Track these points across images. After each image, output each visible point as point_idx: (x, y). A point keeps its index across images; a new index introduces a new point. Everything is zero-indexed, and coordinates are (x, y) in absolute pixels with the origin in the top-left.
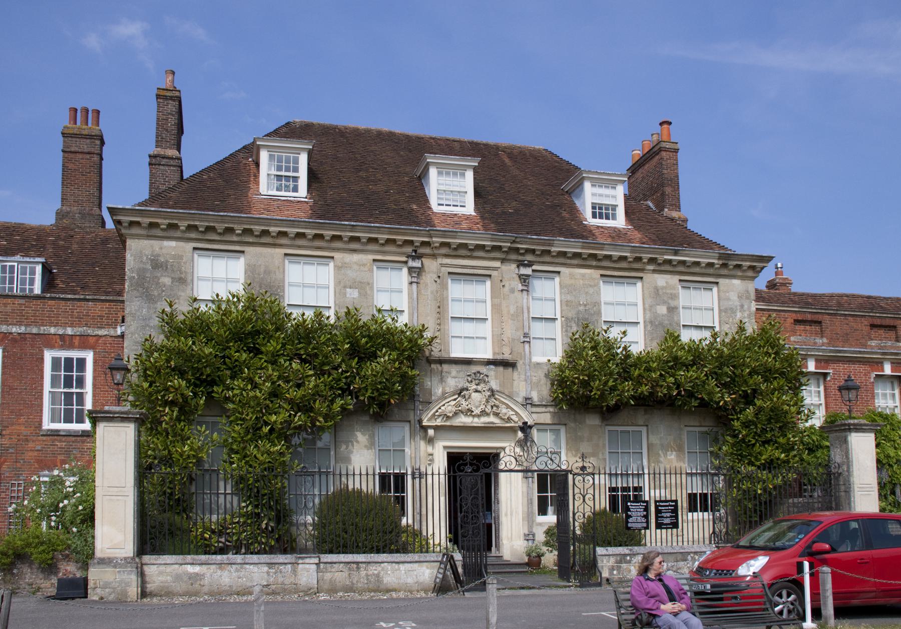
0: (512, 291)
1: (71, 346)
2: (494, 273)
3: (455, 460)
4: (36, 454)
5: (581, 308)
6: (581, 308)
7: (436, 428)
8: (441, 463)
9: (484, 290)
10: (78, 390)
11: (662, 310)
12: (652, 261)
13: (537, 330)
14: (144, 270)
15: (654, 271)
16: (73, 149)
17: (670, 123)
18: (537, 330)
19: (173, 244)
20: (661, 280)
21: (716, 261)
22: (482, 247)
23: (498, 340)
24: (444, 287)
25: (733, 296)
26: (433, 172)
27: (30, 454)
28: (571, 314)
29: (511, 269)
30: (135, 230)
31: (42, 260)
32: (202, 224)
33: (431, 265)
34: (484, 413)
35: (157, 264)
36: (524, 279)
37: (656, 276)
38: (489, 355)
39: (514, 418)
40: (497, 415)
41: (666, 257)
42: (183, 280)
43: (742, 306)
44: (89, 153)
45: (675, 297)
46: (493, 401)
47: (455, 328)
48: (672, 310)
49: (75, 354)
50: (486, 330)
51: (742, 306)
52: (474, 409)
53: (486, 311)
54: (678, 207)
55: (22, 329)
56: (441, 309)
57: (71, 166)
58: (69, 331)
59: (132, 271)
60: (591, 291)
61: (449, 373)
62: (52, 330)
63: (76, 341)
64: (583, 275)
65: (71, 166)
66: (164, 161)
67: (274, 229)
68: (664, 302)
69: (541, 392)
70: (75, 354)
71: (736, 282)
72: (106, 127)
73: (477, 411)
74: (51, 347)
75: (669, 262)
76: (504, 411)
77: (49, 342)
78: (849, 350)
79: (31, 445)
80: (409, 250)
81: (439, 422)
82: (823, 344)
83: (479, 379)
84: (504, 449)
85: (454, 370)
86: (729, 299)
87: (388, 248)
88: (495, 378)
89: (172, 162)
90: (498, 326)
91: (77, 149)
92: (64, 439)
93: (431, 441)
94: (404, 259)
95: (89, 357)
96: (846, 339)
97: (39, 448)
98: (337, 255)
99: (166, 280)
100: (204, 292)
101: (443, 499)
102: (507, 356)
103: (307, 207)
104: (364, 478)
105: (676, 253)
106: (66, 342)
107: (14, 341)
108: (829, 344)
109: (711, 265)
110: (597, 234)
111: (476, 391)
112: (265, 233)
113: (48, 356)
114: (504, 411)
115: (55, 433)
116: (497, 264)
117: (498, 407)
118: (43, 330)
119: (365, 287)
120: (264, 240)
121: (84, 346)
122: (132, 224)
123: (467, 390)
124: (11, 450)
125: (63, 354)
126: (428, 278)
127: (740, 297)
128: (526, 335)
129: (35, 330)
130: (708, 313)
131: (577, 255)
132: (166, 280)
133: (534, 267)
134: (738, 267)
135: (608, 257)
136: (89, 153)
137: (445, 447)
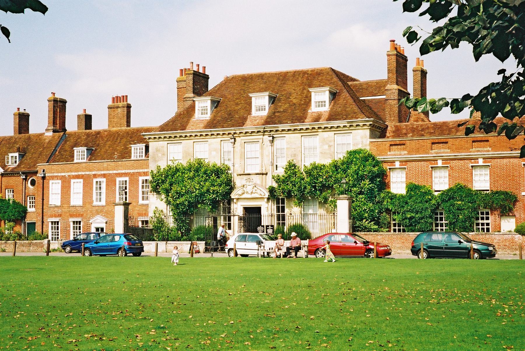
0: (267, 146)
7: (238, 199)
9: (258, 146)
17: (394, 41)
22: (254, 132)
29: (267, 138)
30: (150, 140)
32: (168, 136)
37: (324, 133)
43: (362, 142)
46: (255, 188)
47: (248, 162)
50: (259, 161)
53: (258, 155)
56: (243, 156)
57: (180, 94)
65: (180, 94)
67: (188, 135)
80: (231, 136)
81: (237, 197)
82: (405, 154)
87: (224, 136)
88: (257, 179)
96: (417, 151)
107: (132, 175)
108: (408, 154)
112: (186, 136)
118: (139, 171)
120: (186, 138)
122: (149, 138)
127: (362, 138)
131: (289, 130)
132: (160, 155)
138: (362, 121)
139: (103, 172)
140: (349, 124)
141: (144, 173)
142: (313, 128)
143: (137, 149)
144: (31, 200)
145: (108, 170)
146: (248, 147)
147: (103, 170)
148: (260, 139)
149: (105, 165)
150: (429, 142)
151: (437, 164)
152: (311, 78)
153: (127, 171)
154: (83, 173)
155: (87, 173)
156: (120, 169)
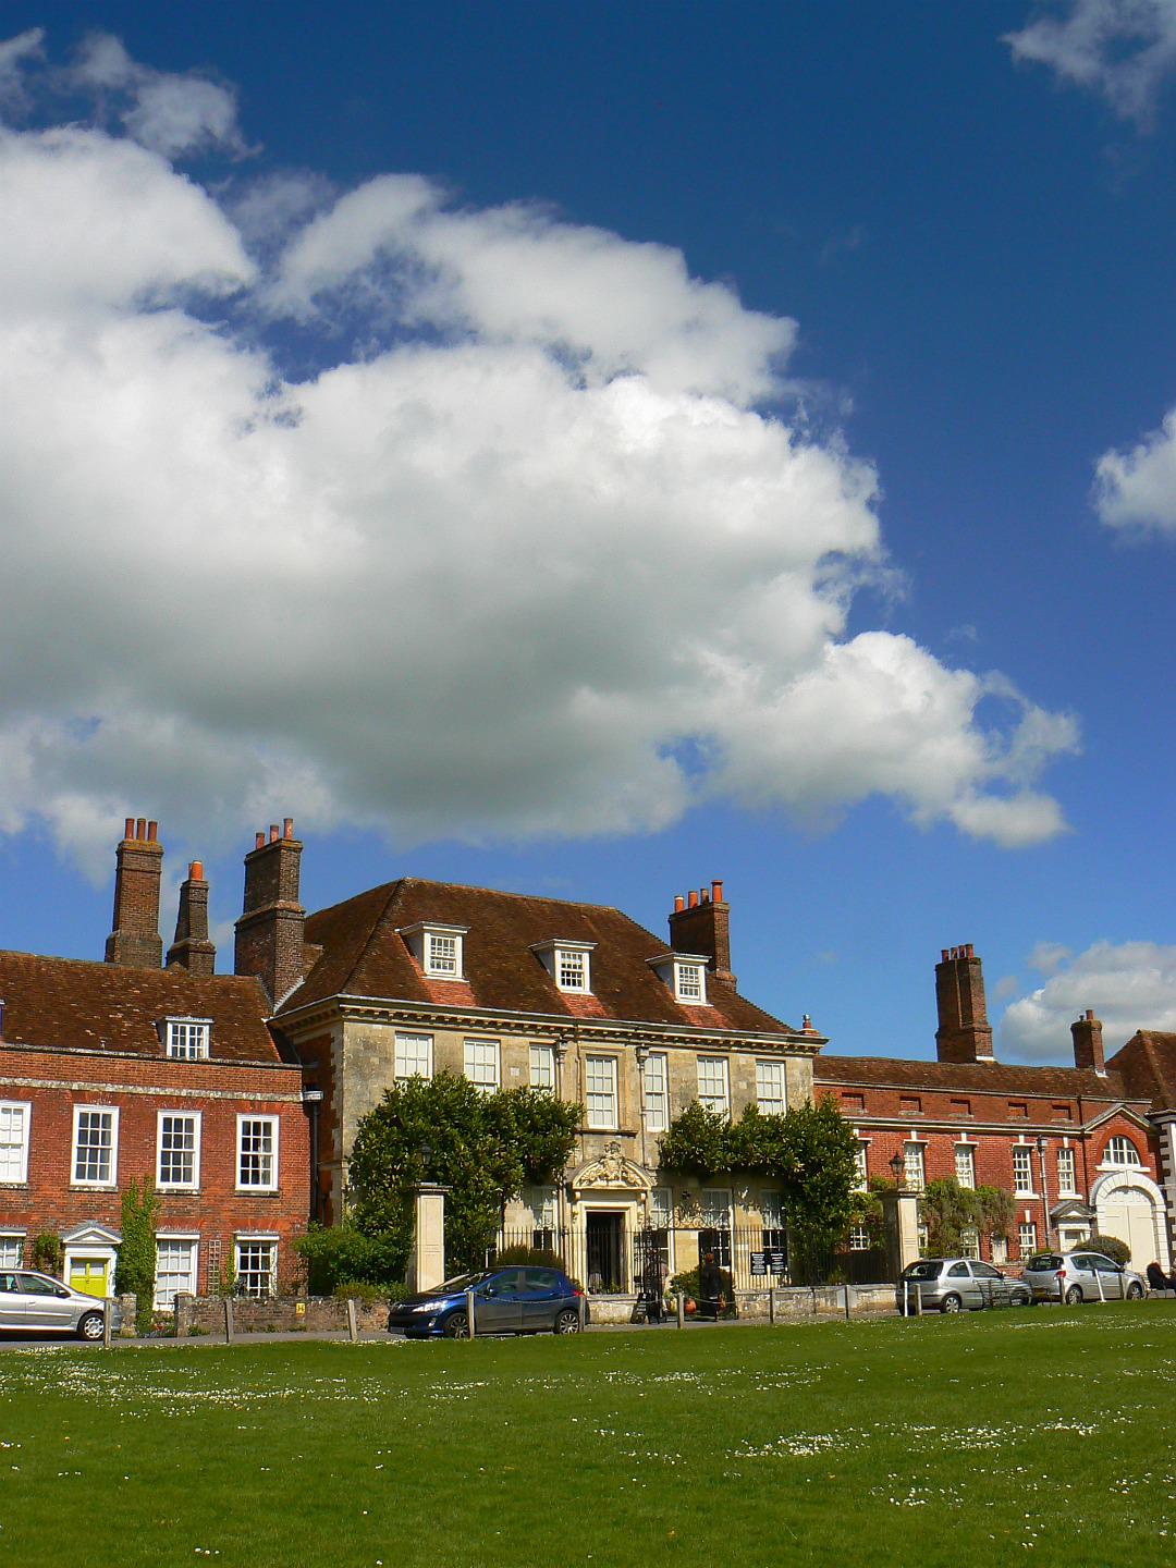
1: (259, 1112)
2: (620, 1055)
3: (594, 1219)
4: (230, 1213)
5: (683, 1085)
6: (683, 1085)
8: (581, 1223)
10: (255, 1153)
11: (743, 1085)
12: (738, 1044)
13: (649, 1102)
14: (358, 1051)
15: (737, 1052)
16: (133, 867)
17: (720, 884)
18: (649, 1102)
19: (380, 1027)
20: (744, 1059)
21: (784, 1043)
23: (622, 1113)
24: (581, 1067)
25: (797, 1073)
26: (558, 953)
27: (225, 1213)
28: (676, 1090)
31: (210, 1021)
33: (570, 1047)
34: (617, 1178)
35: (368, 1046)
36: (640, 1060)
38: (614, 1127)
39: (639, 1182)
40: (624, 1179)
41: (748, 1040)
42: (388, 1060)
43: (803, 1082)
44: (150, 872)
45: (752, 1074)
48: (751, 1085)
49: (262, 1119)
51: (803, 1082)
52: (609, 1174)
54: (728, 967)
55: (218, 1095)
58: (259, 1097)
59: (348, 1051)
60: (690, 1068)
61: (588, 1142)
62: (244, 1096)
63: (264, 1107)
64: (684, 1055)
66: (290, 915)
68: (745, 1079)
69: (653, 1160)
70: (262, 1119)
71: (798, 1059)
72: (160, 840)
73: (612, 1176)
74: (243, 1112)
75: (749, 1045)
76: (632, 1176)
77: (241, 1106)
78: (887, 1120)
79: (226, 1205)
83: (614, 1147)
84: (627, 1208)
85: (592, 1139)
86: (793, 1075)
89: (296, 916)
90: (626, 1100)
91: (137, 867)
92: (253, 1199)
93: (572, 1200)
94: (553, 1041)
95: (275, 1121)
96: (882, 1110)
97: (232, 1208)
98: (503, 1038)
99: (375, 1060)
100: (402, 1069)
101: (585, 1253)
102: (629, 1127)
103: (467, 989)
104: (524, 1236)
105: (756, 1037)
106: (256, 1107)
107: (211, 1105)
109: (781, 1047)
110: (690, 1015)
111: (612, 1159)
113: (240, 1119)
114: (632, 1176)
115: (247, 1194)
116: (621, 1046)
117: (626, 1173)
119: (523, 1066)
121: (270, 1112)
123: (605, 1157)
124: (209, 1211)
125: (253, 1119)
126: (569, 1058)
127: (801, 1074)
128: (643, 1109)
129: (229, 1096)
130: (780, 1088)
131: (682, 1039)
132: (375, 1060)
133: (651, 1049)
134: (802, 1048)
135: (705, 1041)
136: (150, 872)
137: (586, 1208)
138: (724, 1034)
139: (110, 1088)
140: (789, 1044)
141: (252, 1102)
142: (727, 1043)
143: (183, 1031)
144: (1023, 1180)
145: (126, 1083)
146: (591, 1068)
147: (112, 1082)
148: (620, 1051)
149: (119, 1066)
150: (897, 1094)
151: (1018, 1141)
152: (571, 921)
153: (195, 1093)
154: (36, 1084)
155: (54, 1084)
156: (171, 1086)
